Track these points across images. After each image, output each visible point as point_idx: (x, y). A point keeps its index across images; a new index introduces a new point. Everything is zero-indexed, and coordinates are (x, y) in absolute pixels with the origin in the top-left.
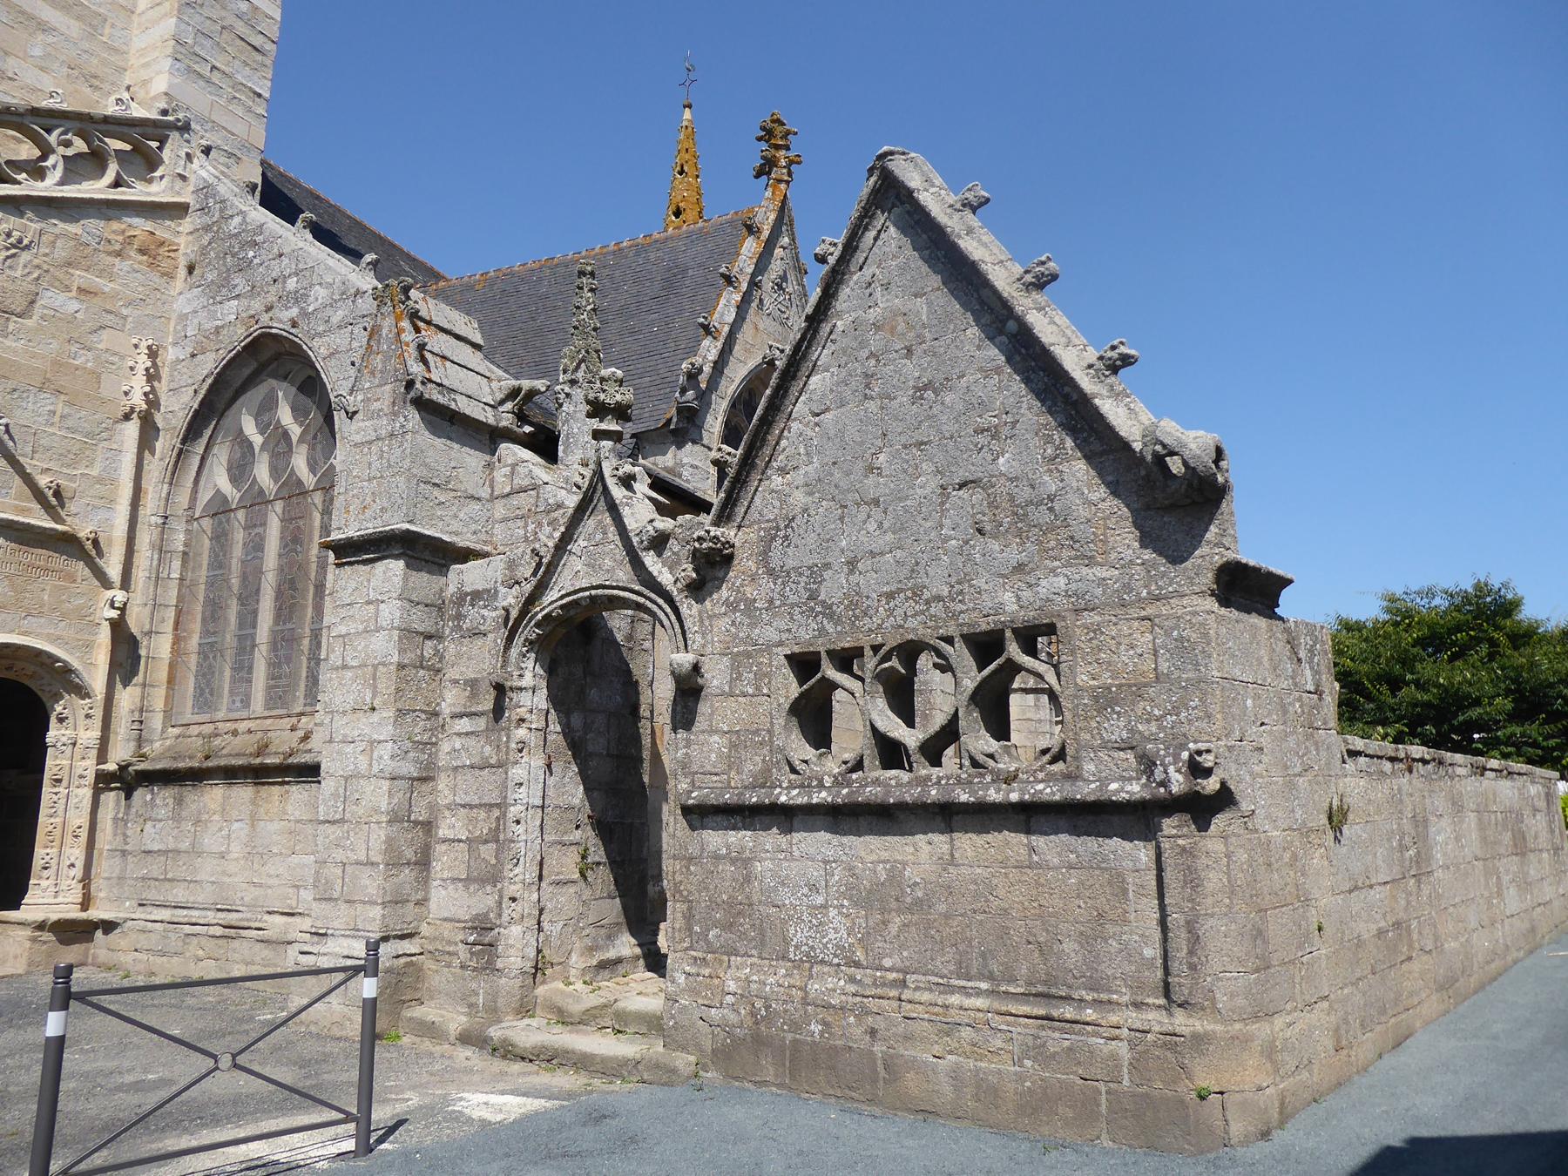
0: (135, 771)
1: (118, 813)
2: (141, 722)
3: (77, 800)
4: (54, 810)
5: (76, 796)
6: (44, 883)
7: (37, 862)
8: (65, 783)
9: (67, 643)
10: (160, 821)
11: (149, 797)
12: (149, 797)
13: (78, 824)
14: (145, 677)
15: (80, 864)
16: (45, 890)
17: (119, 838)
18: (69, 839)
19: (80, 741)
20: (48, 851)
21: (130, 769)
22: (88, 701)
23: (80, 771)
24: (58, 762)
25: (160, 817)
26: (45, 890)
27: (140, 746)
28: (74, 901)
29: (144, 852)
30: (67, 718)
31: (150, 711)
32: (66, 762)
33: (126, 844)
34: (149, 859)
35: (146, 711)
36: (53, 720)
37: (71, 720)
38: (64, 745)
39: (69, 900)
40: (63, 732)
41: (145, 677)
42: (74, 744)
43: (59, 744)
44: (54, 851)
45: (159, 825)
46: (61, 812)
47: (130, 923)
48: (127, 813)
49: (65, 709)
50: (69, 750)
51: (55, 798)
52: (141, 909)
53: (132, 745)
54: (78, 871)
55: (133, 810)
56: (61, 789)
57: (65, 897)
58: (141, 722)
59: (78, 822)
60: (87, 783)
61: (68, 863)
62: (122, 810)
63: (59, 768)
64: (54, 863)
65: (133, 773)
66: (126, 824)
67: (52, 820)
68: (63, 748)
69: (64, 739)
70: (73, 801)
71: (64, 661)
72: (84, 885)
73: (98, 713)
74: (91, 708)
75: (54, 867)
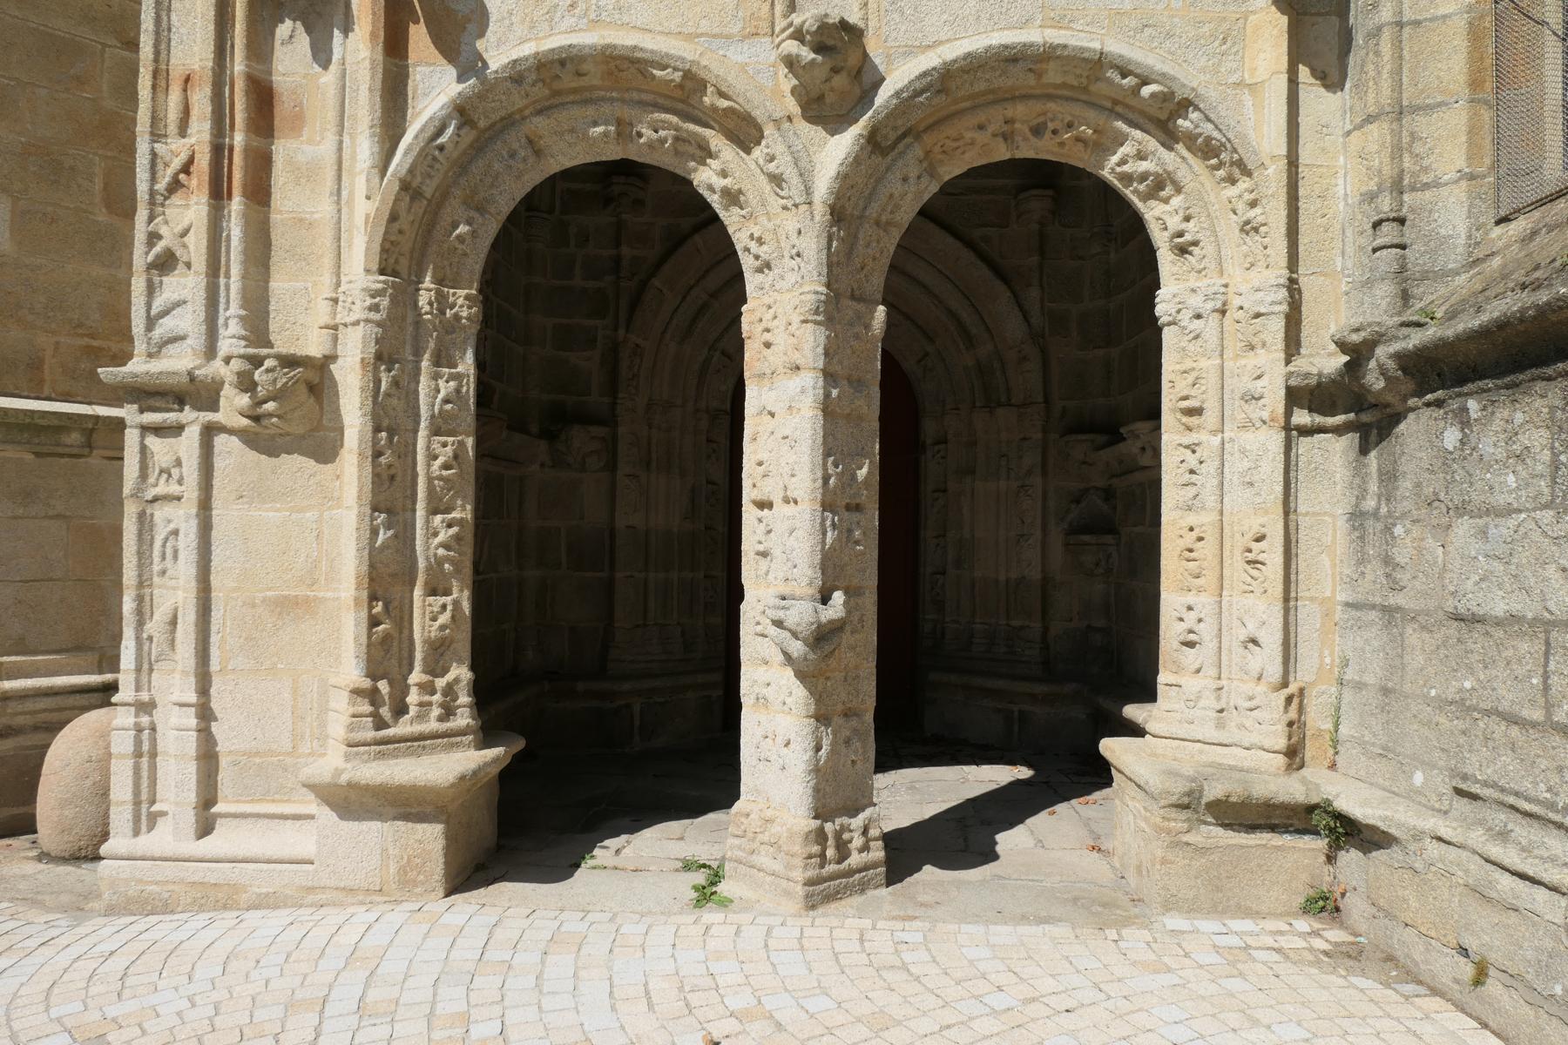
0: (1398, 356)
1: (1361, 497)
2: (1401, 221)
3: (1246, 464)
4: (1192, 491)
5: (1243, 452)
6: (1191, 684)
7: (1170, 630)
8: (1210, 418)
9: (1169, 35)
10: (1509, 511)
11: (1451, 437)
12: (1451, 437)
13: (1256, 530)
14: (1398, 86)
15: (1272, 639)
16: (1192, 702)
17: (1375, 571)
18: (1236, 567)
19: (1236, 302)
20: (1190, 599)
21: (1381, 352)
22: (1244, 184)
23: (1246, 384)
24: (1188, 364)
25: (1501, 499)
26: (1192, 702)
27: (1405, 296)
28: (1267, 744)
29: (1459, 618)
30: (1195, 243)
31: (1426, 186)
32: (1209, 364)
33: (1396, 587)
34: (1477, 642)
35: (1413, 189)
36: (1165, 258)
37: (1207, 247)
38: (1199, 316)
39: (1254, 738)
40: (1192, 284)
41: (1398, 86)
42: (1223, 312)
43: (1185, 317)
44: (1204, 602)
45: (1502, 529)
46: (1211, 500)
47: (1434, 849)
48: (1388, 496)
49: (1187, 219)
50: (1210, 327)
51: (1192, 461)
52: (1463, 805)
53: (1385, 292)
54: (1268, 659)
55: (1405, 485)
56: (1202, 436)
57: (1242, 727)
58: (1401, 221)
59: (1254, 525)
60: (1266, 415)
61: (1243, 634)
62: (1373, 487)
63: (1190, 378)
64: (1206, 631)
65: (1391, 365)
66: (1388, 529)
67: (1192, 519)
68: (1197, 325)
69: (1196, 302)
70: (1236, 466)
71: (1162, 78)
72: (1289, 700)
73: (1275, 214)
74: (1253, 204)
75: (1209, 645)
